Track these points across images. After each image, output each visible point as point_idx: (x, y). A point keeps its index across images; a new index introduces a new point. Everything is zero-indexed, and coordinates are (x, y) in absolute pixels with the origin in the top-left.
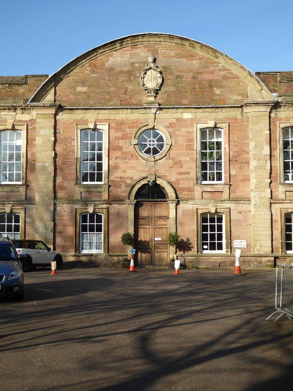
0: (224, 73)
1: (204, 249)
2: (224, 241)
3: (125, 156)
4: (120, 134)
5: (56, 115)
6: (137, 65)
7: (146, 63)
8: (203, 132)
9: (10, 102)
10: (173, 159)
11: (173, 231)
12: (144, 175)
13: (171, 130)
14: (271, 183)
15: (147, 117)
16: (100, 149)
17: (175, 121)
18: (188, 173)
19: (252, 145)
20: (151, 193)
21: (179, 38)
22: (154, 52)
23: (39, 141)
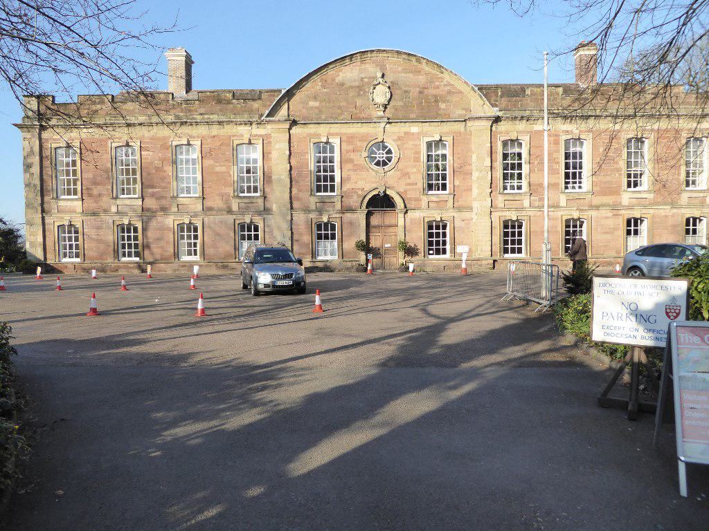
0: (449, 88)
1: (429, 254)
2: (448, 247)
3: (357, 168)
5: (290, 129)
6: (366, 80)
7: (375, 78)
8: (429, 145)
9: (246, 118)
10: (402, 170)
11: (401, 237)
12: (374, 186)
13: (399, 143)
14: (491, 192)
15: (376, 131)
16: (331, 161)
19: (474, 157)
20: (381, 202)
21: (406, 54)
22: (383, 67)
23: (274, 155)
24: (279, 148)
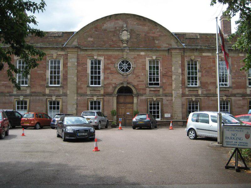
0: (160, 33)
4: (109, 62)
6: (118, 28)
12: (121, 82)
13: (134, 60)
17: (136, 56)
18: (143, 81)
19: (173, 68)
22: (127, 23)
24: (72, 60)
